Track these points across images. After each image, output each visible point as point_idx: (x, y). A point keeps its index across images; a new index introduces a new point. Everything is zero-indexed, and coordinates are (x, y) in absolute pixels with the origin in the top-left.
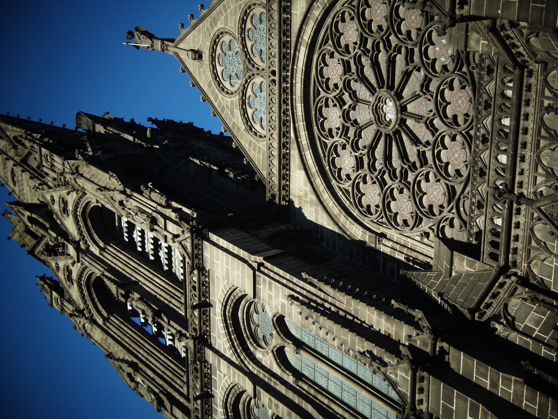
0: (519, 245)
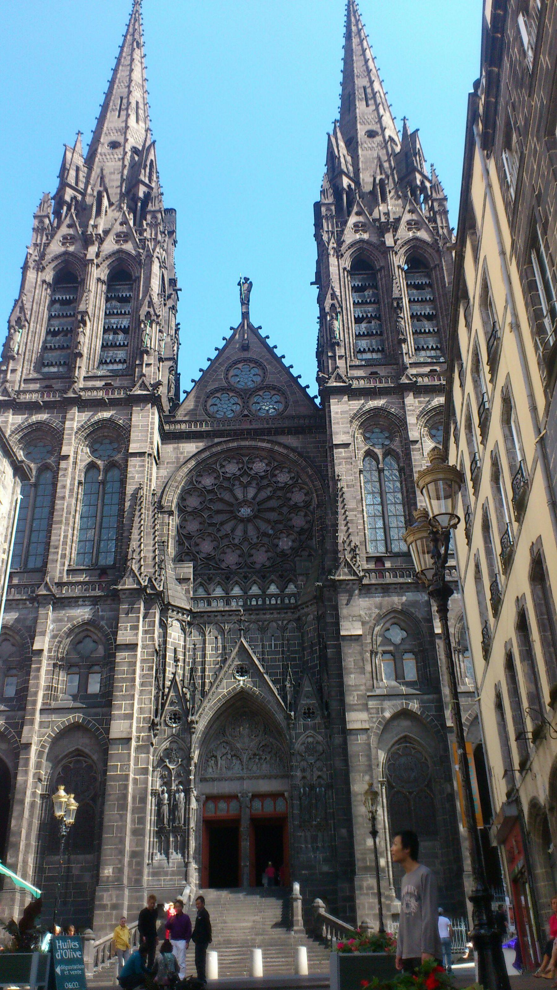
0: (206, 618)
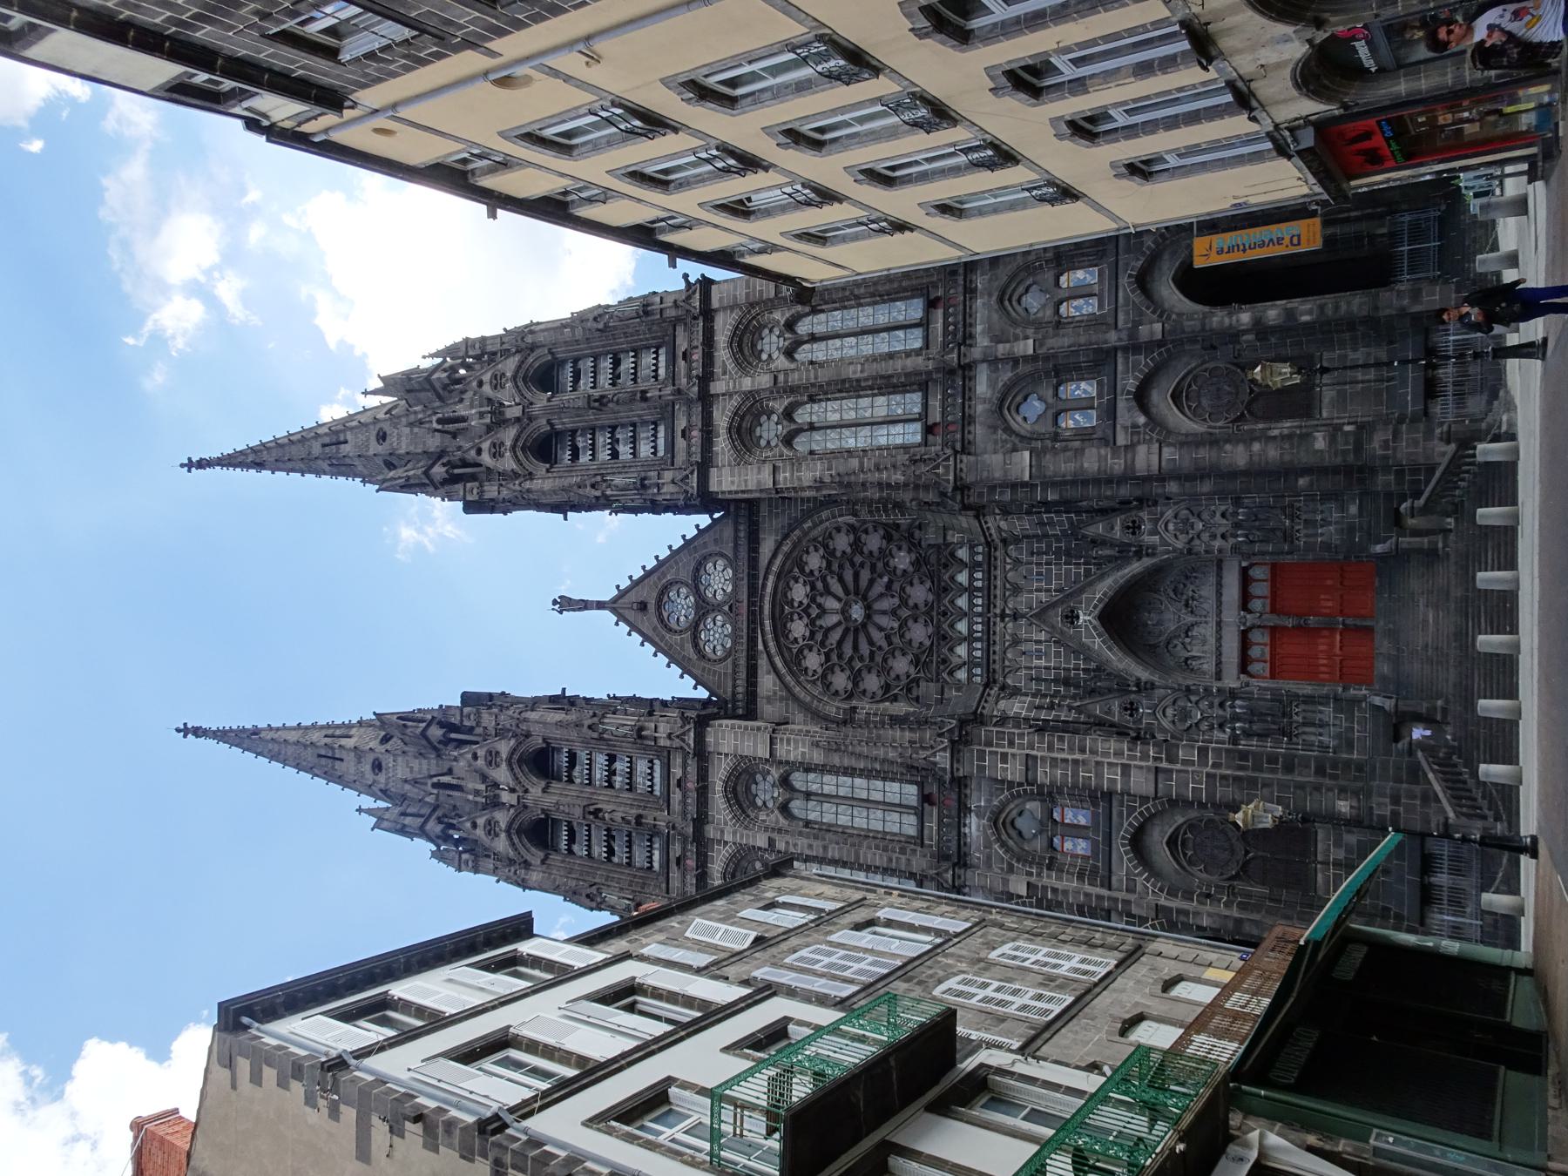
0: (997, 667)
